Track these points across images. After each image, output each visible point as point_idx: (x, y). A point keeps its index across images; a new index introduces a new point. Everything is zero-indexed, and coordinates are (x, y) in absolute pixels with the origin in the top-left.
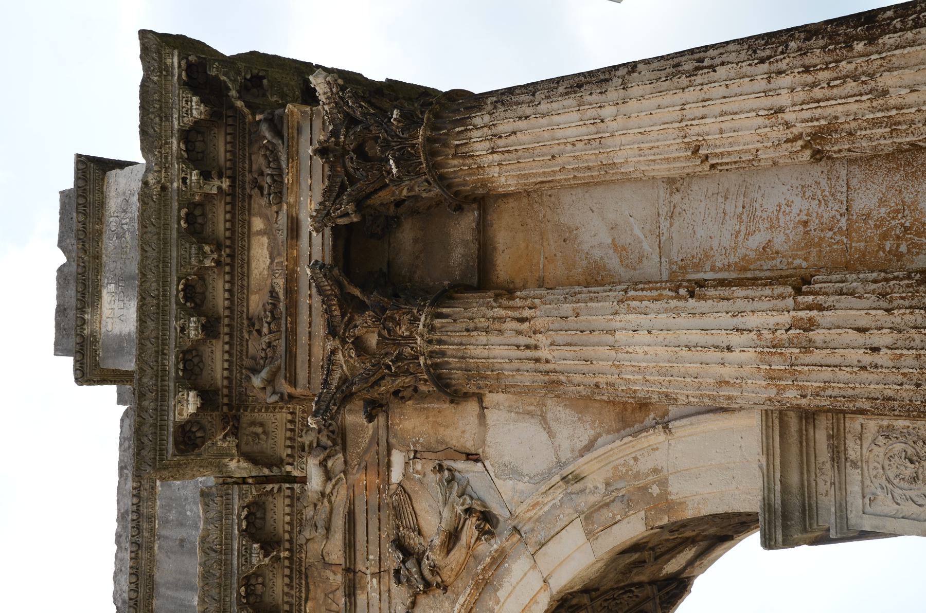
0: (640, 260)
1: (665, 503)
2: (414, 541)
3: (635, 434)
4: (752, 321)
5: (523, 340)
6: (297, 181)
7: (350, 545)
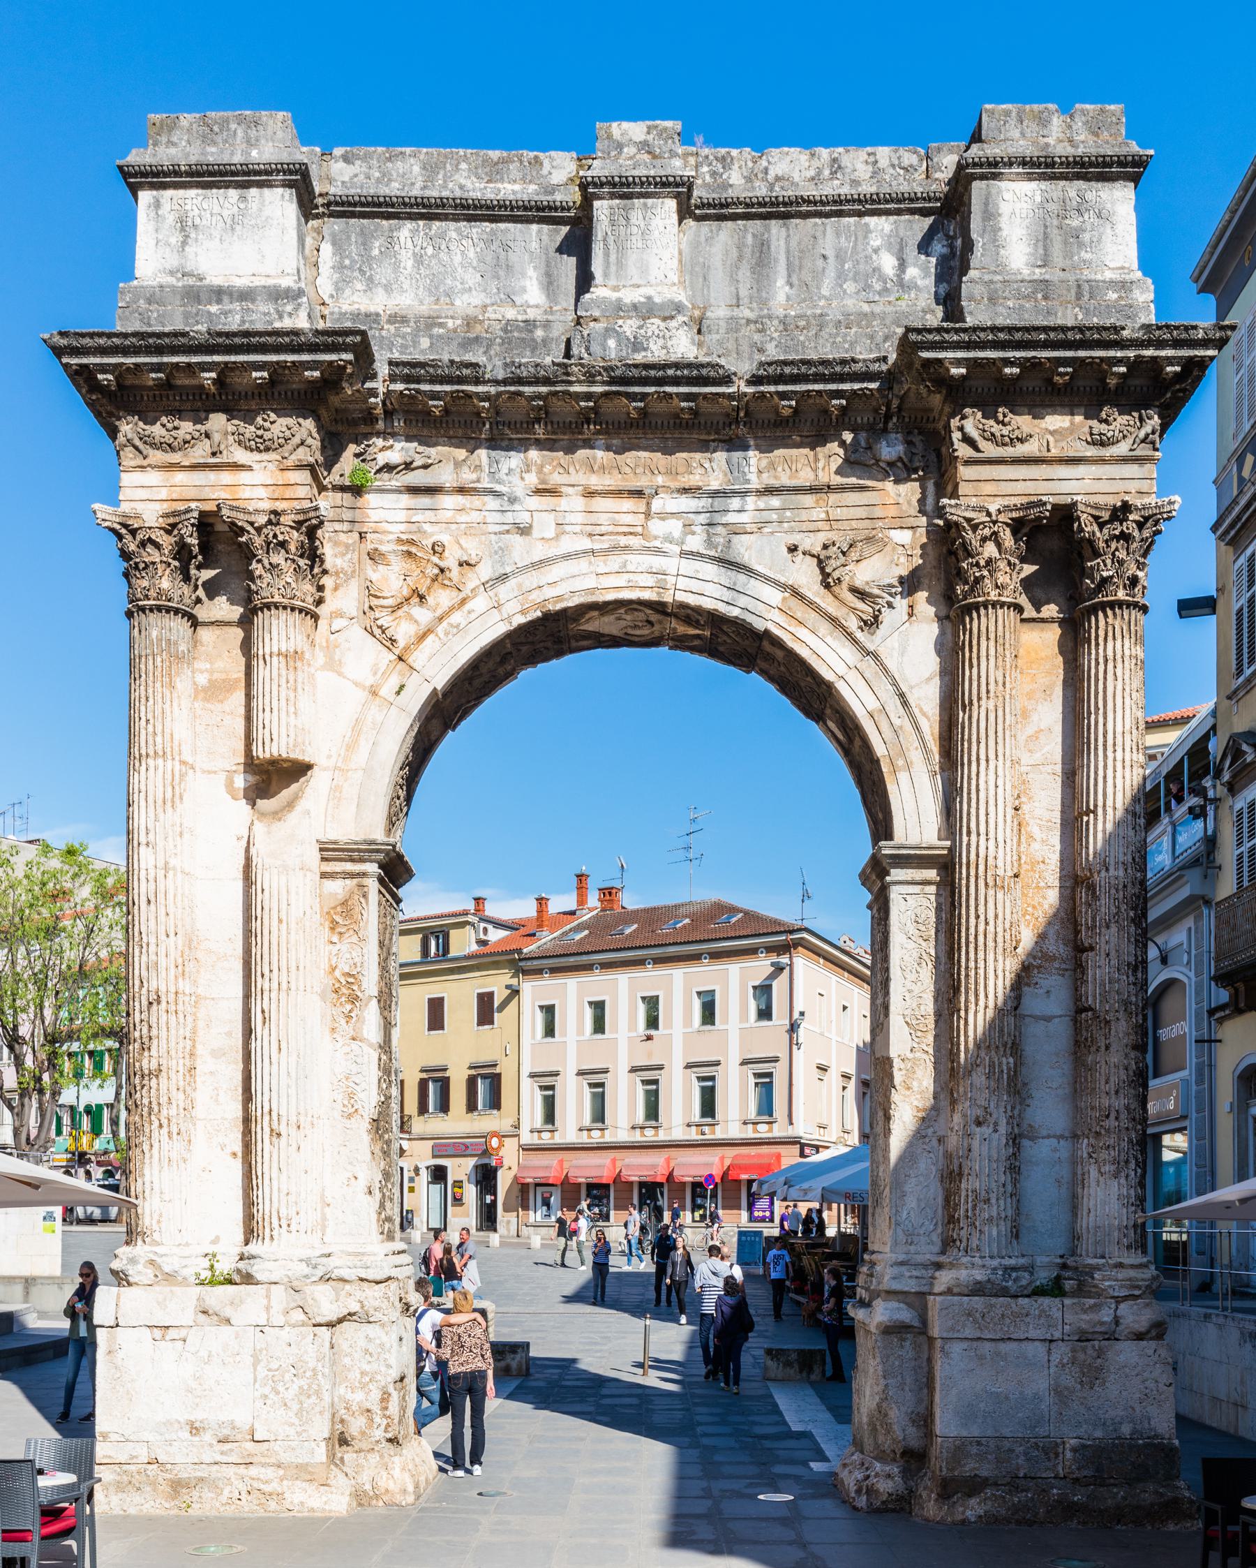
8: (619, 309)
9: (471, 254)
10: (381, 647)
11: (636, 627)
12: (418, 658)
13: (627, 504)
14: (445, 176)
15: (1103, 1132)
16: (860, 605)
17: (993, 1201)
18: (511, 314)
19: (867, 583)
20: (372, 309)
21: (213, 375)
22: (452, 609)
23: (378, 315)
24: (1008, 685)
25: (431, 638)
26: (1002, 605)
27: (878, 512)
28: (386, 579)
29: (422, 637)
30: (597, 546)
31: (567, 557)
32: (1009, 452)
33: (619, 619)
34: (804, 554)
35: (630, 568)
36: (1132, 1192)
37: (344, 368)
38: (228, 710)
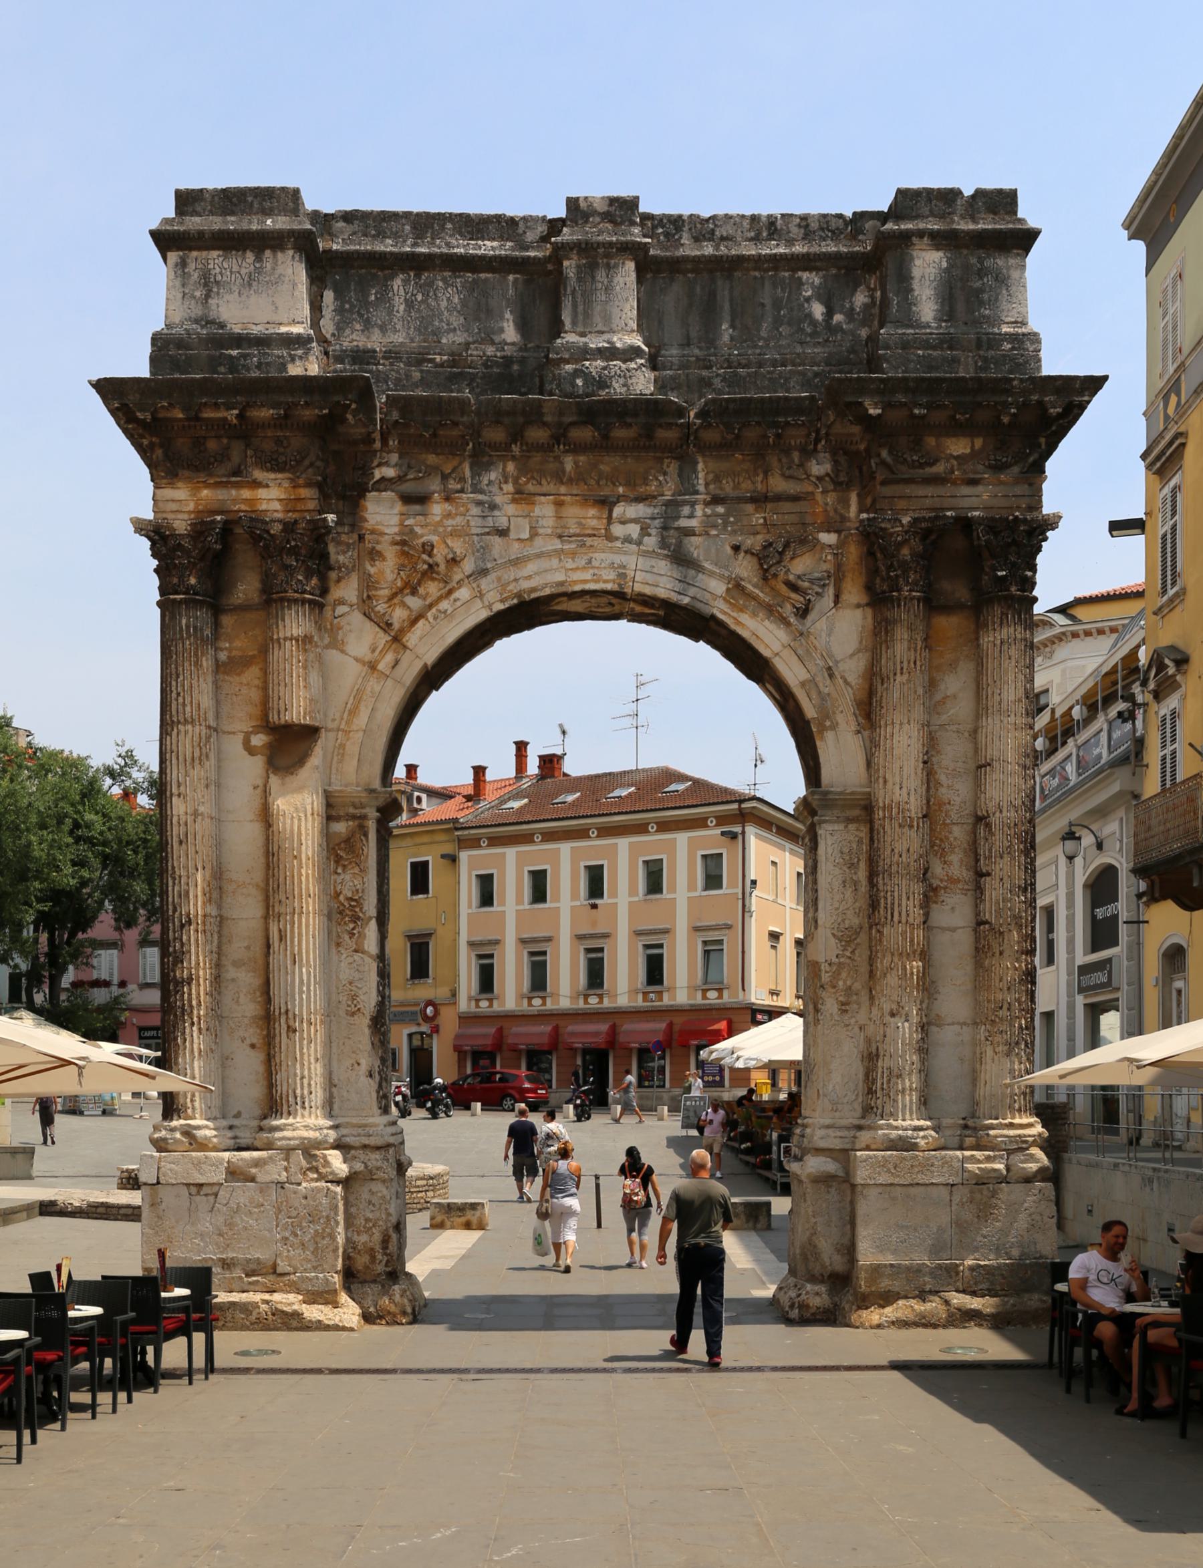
0: (938, 714)
1: (823, 729)
2: (789, 554)
3: (854, 714)
4: (912, 798)
5: (905, 665)
6: (1001, 483)
7: (778, 498)
8: (585, 353)
9: (456, 300)
10: (378, 629)
11: (598, 607)
12: (412, 638)
13: (592, 512)
14: (433, 233)
16: (793, 595)
18: (490, 351)
19: (799, 577)
23: (375, 351)
28: (382, 572)
29: (414, 622)
31: (539, 556)
34: (746, 552)
38: (245, 681)
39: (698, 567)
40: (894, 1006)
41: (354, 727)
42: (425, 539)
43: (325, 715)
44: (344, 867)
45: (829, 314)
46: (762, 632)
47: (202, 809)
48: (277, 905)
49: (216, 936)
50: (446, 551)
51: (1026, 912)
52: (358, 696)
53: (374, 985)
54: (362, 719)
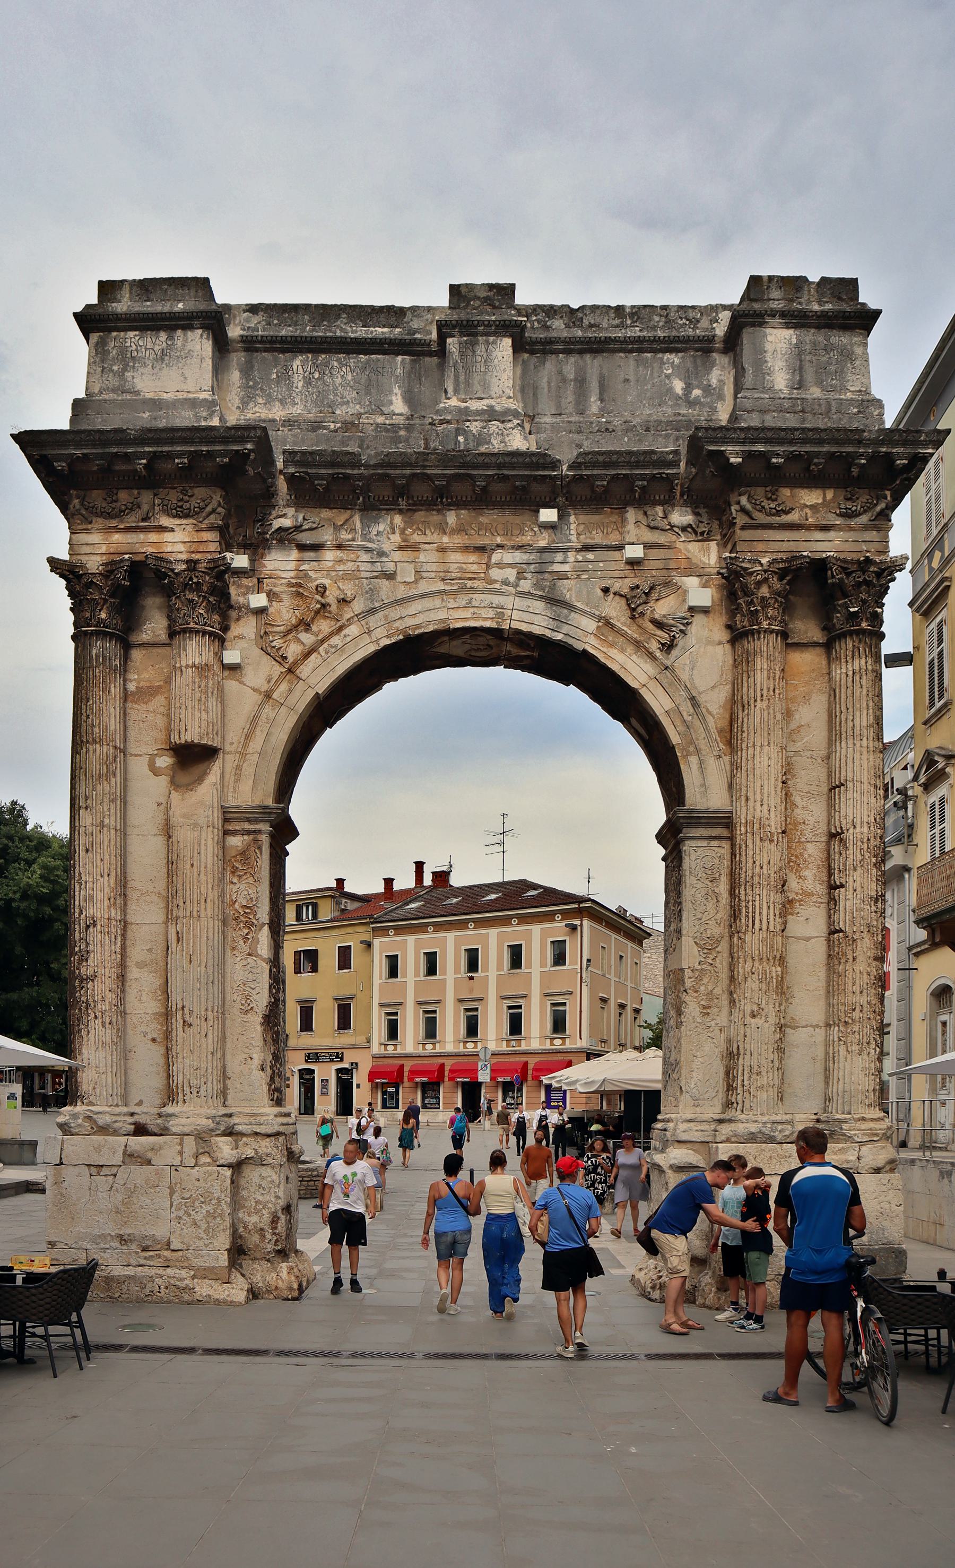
2: (654, 596)
9: (349, 377)
10: (274, 663)
12: (304, 670)
13: (473, 558)
15: (850, 1021)
16: (659, 632)
17: (764, 1073)
18: (380, 419)
19: (664, 616)
20: (270, 416)
21: (144, 461)
22: (332, 634)
24: (777, 691)
25: (314, 655)
26: (772, 631)
27: (672, 565)
28: (279, 612)
29: (307, 655)
30: (448, 588)
31: (423, 596)
32: (777, 519)
33: (464, 643)
34: (615, 594)
35: (475, 603)
36: (872, 1065)
37: (248, 455)
39: (571, 607)
40: (755, 1008)
41: (250, 750)
42: (318, 582)
43: (223, 738)
44: (240, 876)
45: (688, 388)
46: (630, 665)
47: (107, 821)
48: (175, 909)
49: (119, 938)
50: (338, 592)
51: (877, 920)
52: (254, 721)
53: (267, 986)
54: (256, 744)
